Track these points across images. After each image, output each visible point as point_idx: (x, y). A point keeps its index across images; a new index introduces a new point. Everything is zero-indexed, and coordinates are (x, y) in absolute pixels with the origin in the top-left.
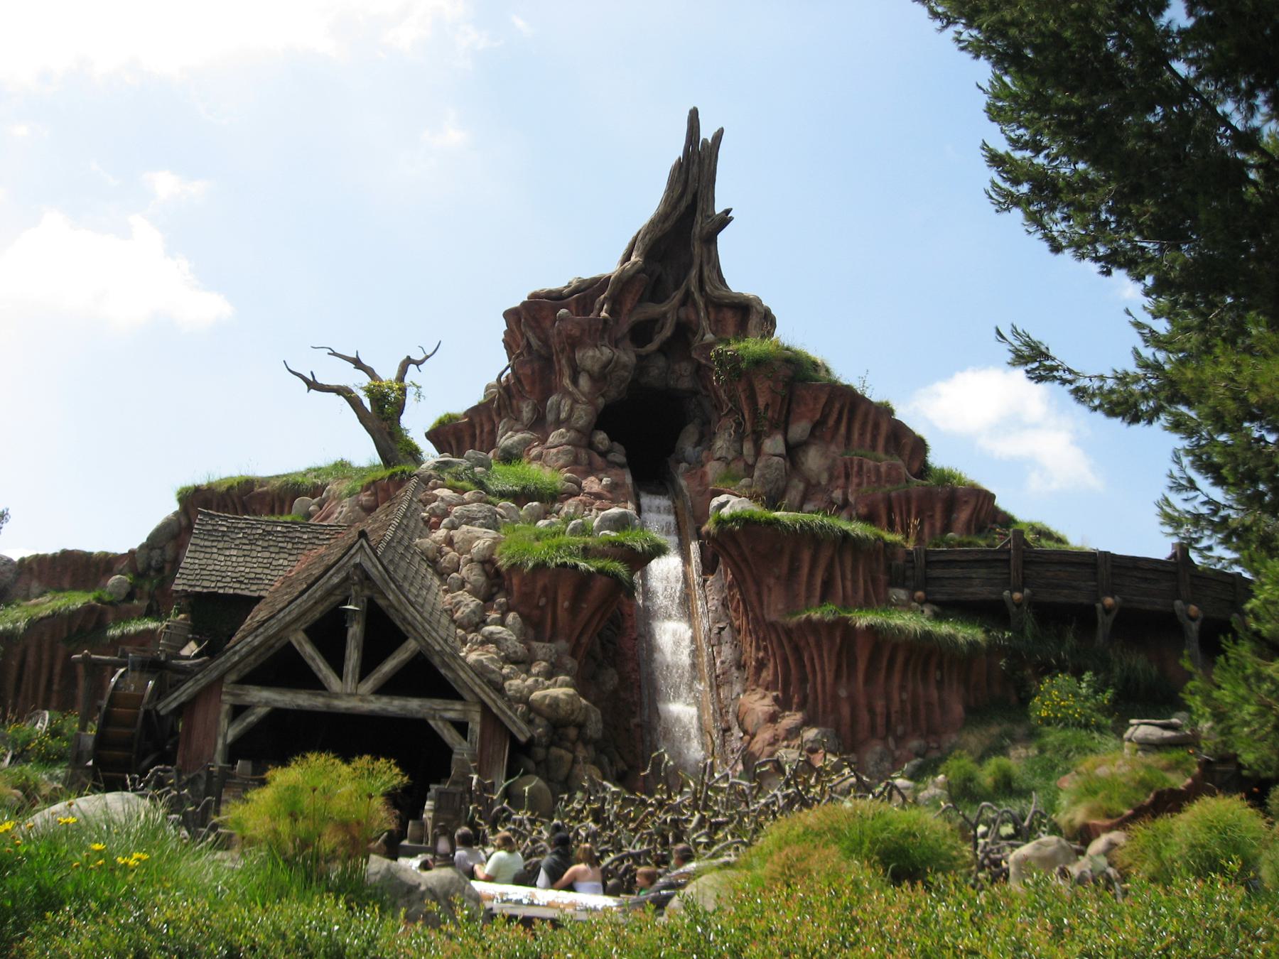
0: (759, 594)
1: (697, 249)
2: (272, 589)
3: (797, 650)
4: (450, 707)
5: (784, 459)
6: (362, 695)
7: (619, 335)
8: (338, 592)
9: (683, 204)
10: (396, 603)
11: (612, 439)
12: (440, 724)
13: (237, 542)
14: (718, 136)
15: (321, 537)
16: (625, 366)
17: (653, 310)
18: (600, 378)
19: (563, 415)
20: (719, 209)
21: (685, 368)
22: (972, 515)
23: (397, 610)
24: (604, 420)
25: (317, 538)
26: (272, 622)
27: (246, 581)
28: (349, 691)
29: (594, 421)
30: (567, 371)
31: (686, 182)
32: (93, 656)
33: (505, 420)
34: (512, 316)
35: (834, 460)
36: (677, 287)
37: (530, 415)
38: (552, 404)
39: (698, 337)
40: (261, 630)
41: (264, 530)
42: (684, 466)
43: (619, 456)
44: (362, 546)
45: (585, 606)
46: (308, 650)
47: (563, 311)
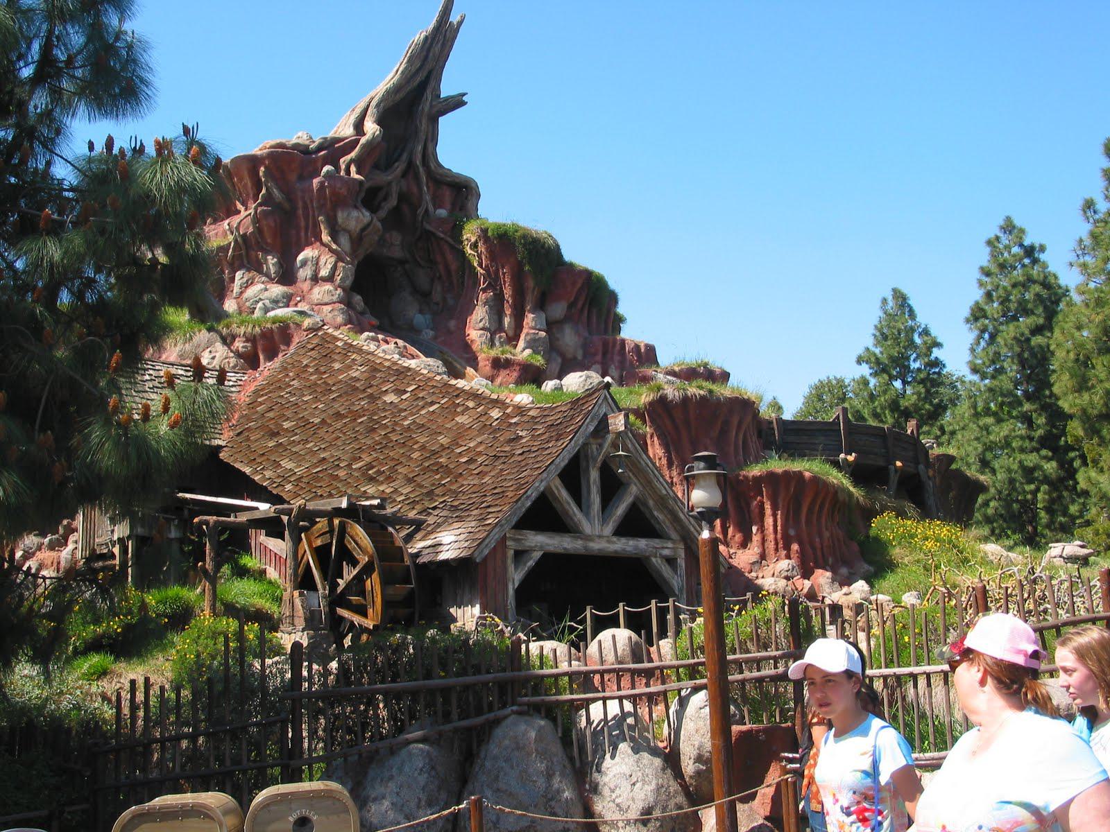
9: (418, 79)
31: (426, 57)
46: (564, 494)
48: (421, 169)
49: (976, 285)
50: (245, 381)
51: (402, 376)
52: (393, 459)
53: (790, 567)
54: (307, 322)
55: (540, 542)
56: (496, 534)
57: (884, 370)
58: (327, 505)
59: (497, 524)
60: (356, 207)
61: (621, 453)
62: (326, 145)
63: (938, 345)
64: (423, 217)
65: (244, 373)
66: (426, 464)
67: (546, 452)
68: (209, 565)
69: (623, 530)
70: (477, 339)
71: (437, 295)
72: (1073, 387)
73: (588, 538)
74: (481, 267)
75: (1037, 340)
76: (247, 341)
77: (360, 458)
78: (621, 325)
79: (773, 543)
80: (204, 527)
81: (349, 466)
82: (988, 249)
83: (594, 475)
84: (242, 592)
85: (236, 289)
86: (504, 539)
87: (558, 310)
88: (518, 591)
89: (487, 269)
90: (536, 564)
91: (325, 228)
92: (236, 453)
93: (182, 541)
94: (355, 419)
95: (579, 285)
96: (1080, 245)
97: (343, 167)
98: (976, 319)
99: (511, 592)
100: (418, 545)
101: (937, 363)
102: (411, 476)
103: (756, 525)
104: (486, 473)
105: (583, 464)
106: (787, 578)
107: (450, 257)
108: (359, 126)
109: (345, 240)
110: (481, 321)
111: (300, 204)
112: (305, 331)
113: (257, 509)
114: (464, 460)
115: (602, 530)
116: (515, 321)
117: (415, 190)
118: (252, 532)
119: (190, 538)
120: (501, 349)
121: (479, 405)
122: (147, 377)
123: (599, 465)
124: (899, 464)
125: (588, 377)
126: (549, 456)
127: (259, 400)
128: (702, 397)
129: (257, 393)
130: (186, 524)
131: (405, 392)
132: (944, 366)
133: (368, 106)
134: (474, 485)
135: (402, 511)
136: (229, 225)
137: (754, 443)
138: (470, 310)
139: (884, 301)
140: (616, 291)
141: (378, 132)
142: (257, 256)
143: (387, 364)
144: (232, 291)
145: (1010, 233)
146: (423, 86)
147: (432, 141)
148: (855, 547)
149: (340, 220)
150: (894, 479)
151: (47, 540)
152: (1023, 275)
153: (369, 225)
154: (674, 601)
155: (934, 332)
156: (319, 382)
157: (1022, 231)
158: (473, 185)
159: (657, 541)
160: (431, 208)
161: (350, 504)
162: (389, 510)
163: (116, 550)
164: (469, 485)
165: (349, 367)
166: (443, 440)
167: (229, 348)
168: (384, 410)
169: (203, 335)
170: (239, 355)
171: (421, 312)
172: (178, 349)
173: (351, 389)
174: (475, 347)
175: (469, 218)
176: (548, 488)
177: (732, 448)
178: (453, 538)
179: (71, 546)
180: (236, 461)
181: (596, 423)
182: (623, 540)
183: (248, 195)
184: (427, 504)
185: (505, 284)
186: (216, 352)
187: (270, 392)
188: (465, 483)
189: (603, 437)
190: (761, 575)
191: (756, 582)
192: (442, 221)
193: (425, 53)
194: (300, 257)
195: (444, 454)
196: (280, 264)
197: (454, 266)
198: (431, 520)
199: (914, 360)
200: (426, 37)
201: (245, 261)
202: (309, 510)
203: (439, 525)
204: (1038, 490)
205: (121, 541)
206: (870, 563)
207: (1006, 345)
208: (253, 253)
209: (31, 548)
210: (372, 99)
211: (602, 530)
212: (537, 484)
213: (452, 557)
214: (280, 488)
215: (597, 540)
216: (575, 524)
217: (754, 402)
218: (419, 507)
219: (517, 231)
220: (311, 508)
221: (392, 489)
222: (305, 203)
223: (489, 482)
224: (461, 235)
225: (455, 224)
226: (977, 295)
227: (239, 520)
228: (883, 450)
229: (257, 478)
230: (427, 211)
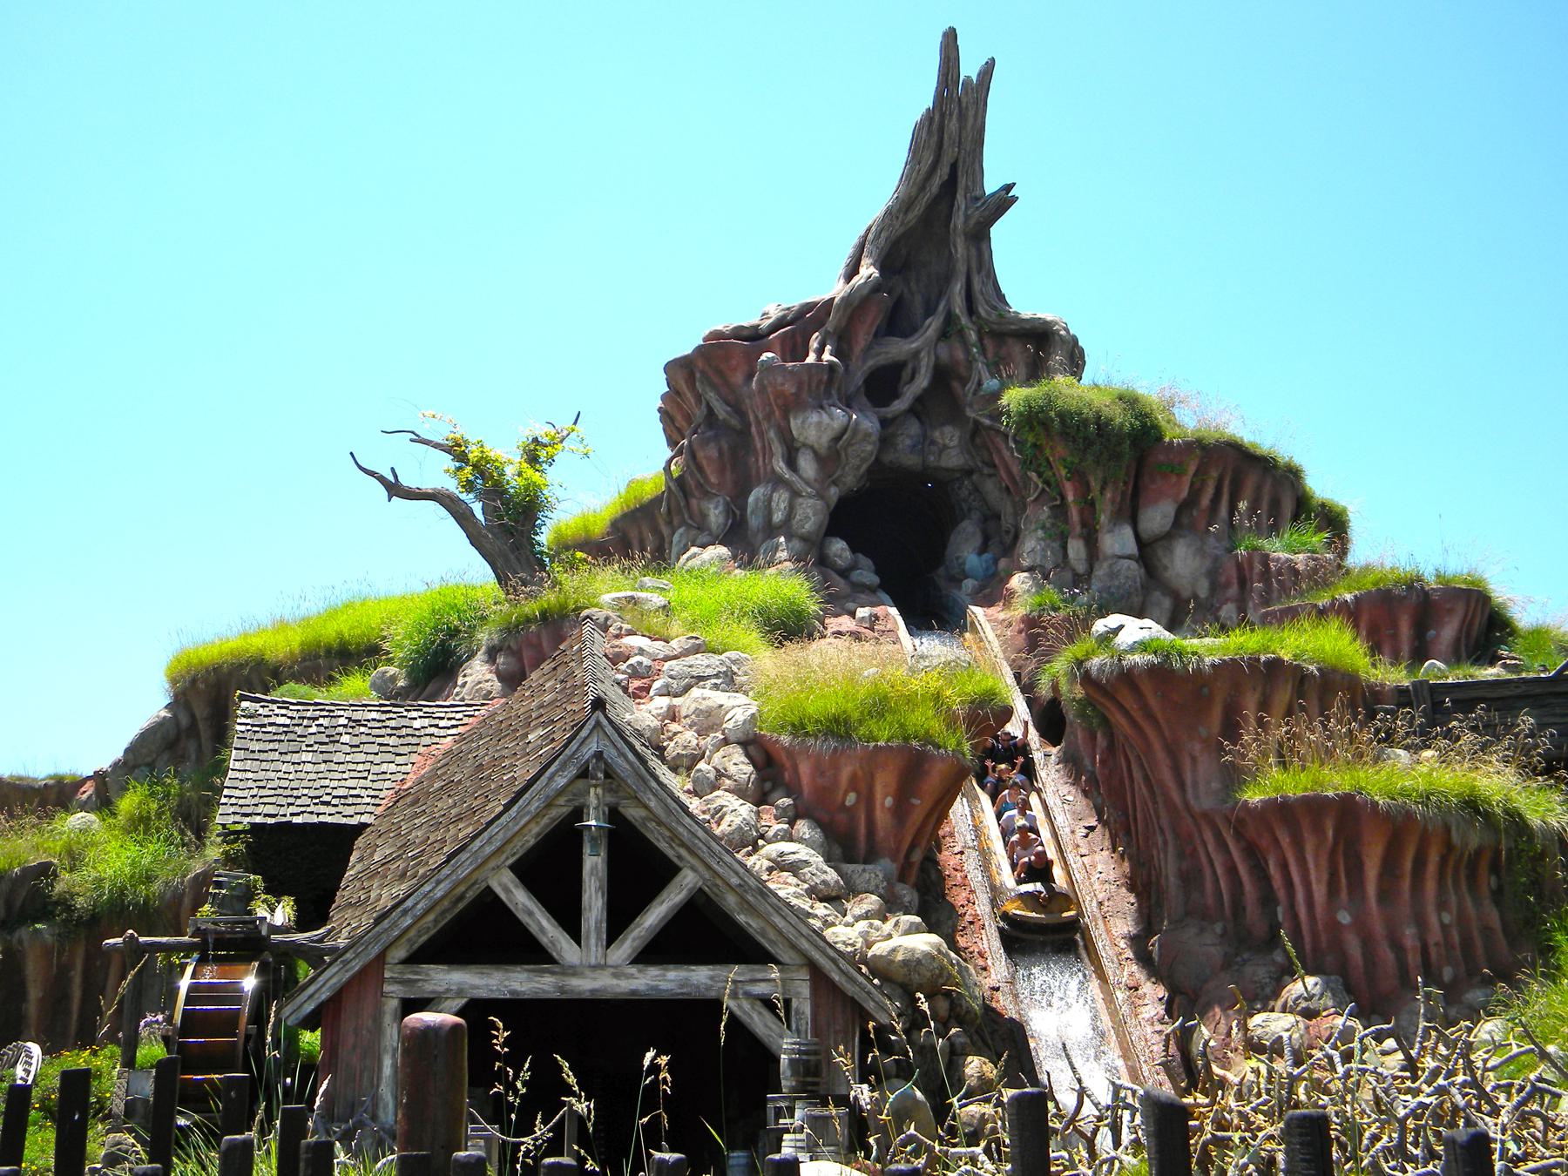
0: (1177, 771)
1: (960, 248)
2: (379, 811)
3: (1253, 852)
4: (759, 976)
5: (1137, 562)
6: (615, 967)
7: (852, 389)
8: (562, 801)
9: (936, 182)
10: (660, 812)
11: (854, 549)
12: (746, 1005)
13: (311, 740)
14: (988, 70)
15: (442, 723)
16: (867, 435)
17: (898, 348)
18: (829, 460)
19: (778, 517)
20: (991, 185)
21: (949, 436)
22: (1460, 630)
23: (660, 823)
24: (841, 520)
25: (436, 726)
26: (463, 856)
27: (334, 802)
28: (593, 961)
29: (826, 523)
30: (778, 449)
32: (142, 939)
33: (681, 530)
34: (681, 371)
35: (1216, 559)
36: (930, 311)
37: (721, 520)
38: (757, 500)
39: (971, 386)
40: (446, 871)
41: (349, 719)
42: (969, 584)
43: (868, 575)
44: (598, 724)
45: (916, 802)
46: (520, 900)
47: (766, 356)
182: (653, 971)
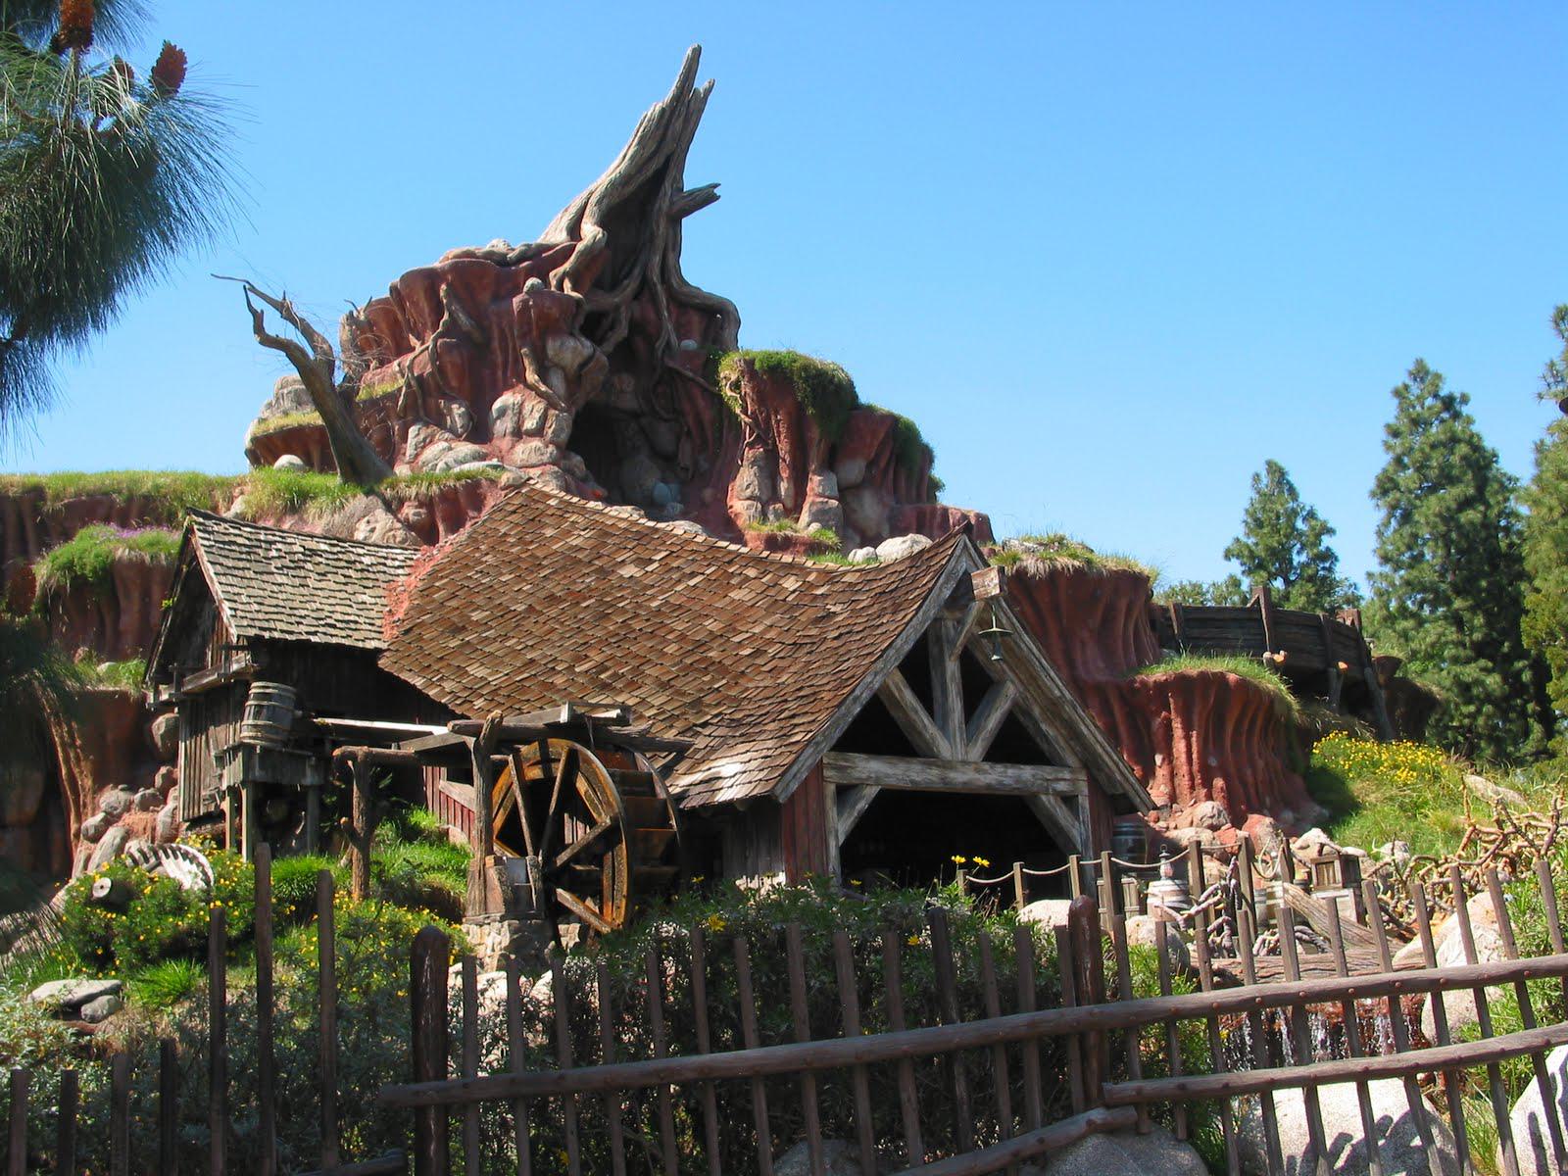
9: (654, 166)
12: (1052, 798)
46: (908, 697)
48: (659, 287)
49: (1381, 449)
50: (417, 560)
51: (648, 539)
52: (637, 656)
53: (1215, 811)
54: (505, 478)
55: (876, 771)
56: (808, 759)
57: (1261, 566)
58: (536, 718)
59: (809, 741)
60: (572, 334)
61: (995, 629)
62: (530, 254)
63: (1331, 531)
64: (664, 351)
65: (416, 550)
66: (688, 661)
67: (879, 631)
68: (358, 823)
69: (998, 752)
70: (744, 512)
71: (685, 457)
72: (1559, 557)
73: (947, 765)
74: (746, 414)
75: (1472, 516)
76: (421, 505)
77: (586, 656)
78: (937, 494)
79: (1186, 778)
80: (350, 763)
81: (571, 668)
82: (1396, 401)
83: (952, 667)
84: (399, 858)
85: (410, 449)
86: (819, 767)
87: (854, 470)
88: (844, 850)
89: (754, 417)
90: (871, 806)
91: (530, 364)
92: (402, 658)
93: (323, 788)
94: (578, 603)
95: (881, 436)
96: (1552, 371)
97: (554, 282)
98: (1385, 492)
99: (833, 851)
100: (681, 782)
101: (1328, 556)
102: (665, 679)
103: (1161, 753)
104: (783, 670)
105: (934, 650)
106: (1214, 828)
107: (701, 403)
108: (574, 231)
109: (557, 380)
110: (748, 487)
111: (496, 334)
112: (502, 489)
113: (431, 733)
114: (748, 651)
115: (966, 753)
116: (795, 485)
117: (652, 316)
118: (428, 771)
119: (333, 784)
120: (777, 524)
121: (765, 573)
122: (274, 553)
123: (958, 650)
124: (1342, 665)
125: (915, 542)
126: (884, 637)
127: (437, 584)
128: (1077, 570)
129: (433, 575)
130: (325, 763)
131: (651, 561)
132: (1336, 559)
133: (586, 204)
134: (766, 687)
135: (653, 730)
136: (399, 365)
137: (1148, 638)
138: (732, 473)
139: (1257, 477)
140: (931, 446)
141: (600, 235)
142: (438, 405)
143: (622, 525)
144: (404, 454)
145: (1422, 380)
146: (659, 177)
147: (674, 250)
148: (1298, 781)
149: (550, 353)
150: (1336, 686)
151: (137, 797)
152: (1445, 433)
153: (590, 358)
154: (1110, 856)
155: (1321, 515)
156: (523, 556)
157: (1438, 376)
158: (731, 309)
159: (1048, 769)
160: (674, 338)
161: (573, 715)
162: (635, 728)
163: (226, 806)
164: (758, 687)
165: (569, 533)
166: (711, 625)
167: (395, 516)
168: (621, 588)
169: (359, 501)
170: (408, 525)
171: (664, 480)
172: (324, 521)
173: (571, 562)
174: (740, 523)
175: (725, 352)
176: (884, 687)
177: (1120, 643)
178: (739, 768)
179: (171, 804)
180: (402, 669)
181: (953, 584)
182: (999, 768)
183: (424, 325)
184: (693, 720)
185: (779, 436)
186: (377, 521)
187: (453, 573)
188: (750, 685)
189: (965, 608)
190: (1172, 825)
191: (1167, 834)
192: (689, 355)
193: (660, 132)
194: (497, 405)
195: (715, 646)
196: (469, 416)
197: (708, 415)
198: (700, 742)
199: (1299, 553)
200: (663, 110)
201: (422, 413)
202: (508, 727)
203: (714, 750)
204: (1479, 711)
205: (234, 792)
206: (1322, 803)
207: (1428, 523)
208: (431, 401)
209: (116, 809)
210: (591, 193)
211: (966, 753)
212: (869, 679)
213: (739, 796)
214: (467, 706)
215: (959, 766)
216: (925, 741)
217: (1148, 578)
218: (679, 725)
219: (795, 361)
220: (512, 724)
221: (638, 700)
222: (502, 331)
223: (790, 681)
224: (717, 372)
225: (708, 359)
226: (1382, 460)
227: (402, 751)
228: (1319, 648)
229: (432, 693)
230: (668, 344)
